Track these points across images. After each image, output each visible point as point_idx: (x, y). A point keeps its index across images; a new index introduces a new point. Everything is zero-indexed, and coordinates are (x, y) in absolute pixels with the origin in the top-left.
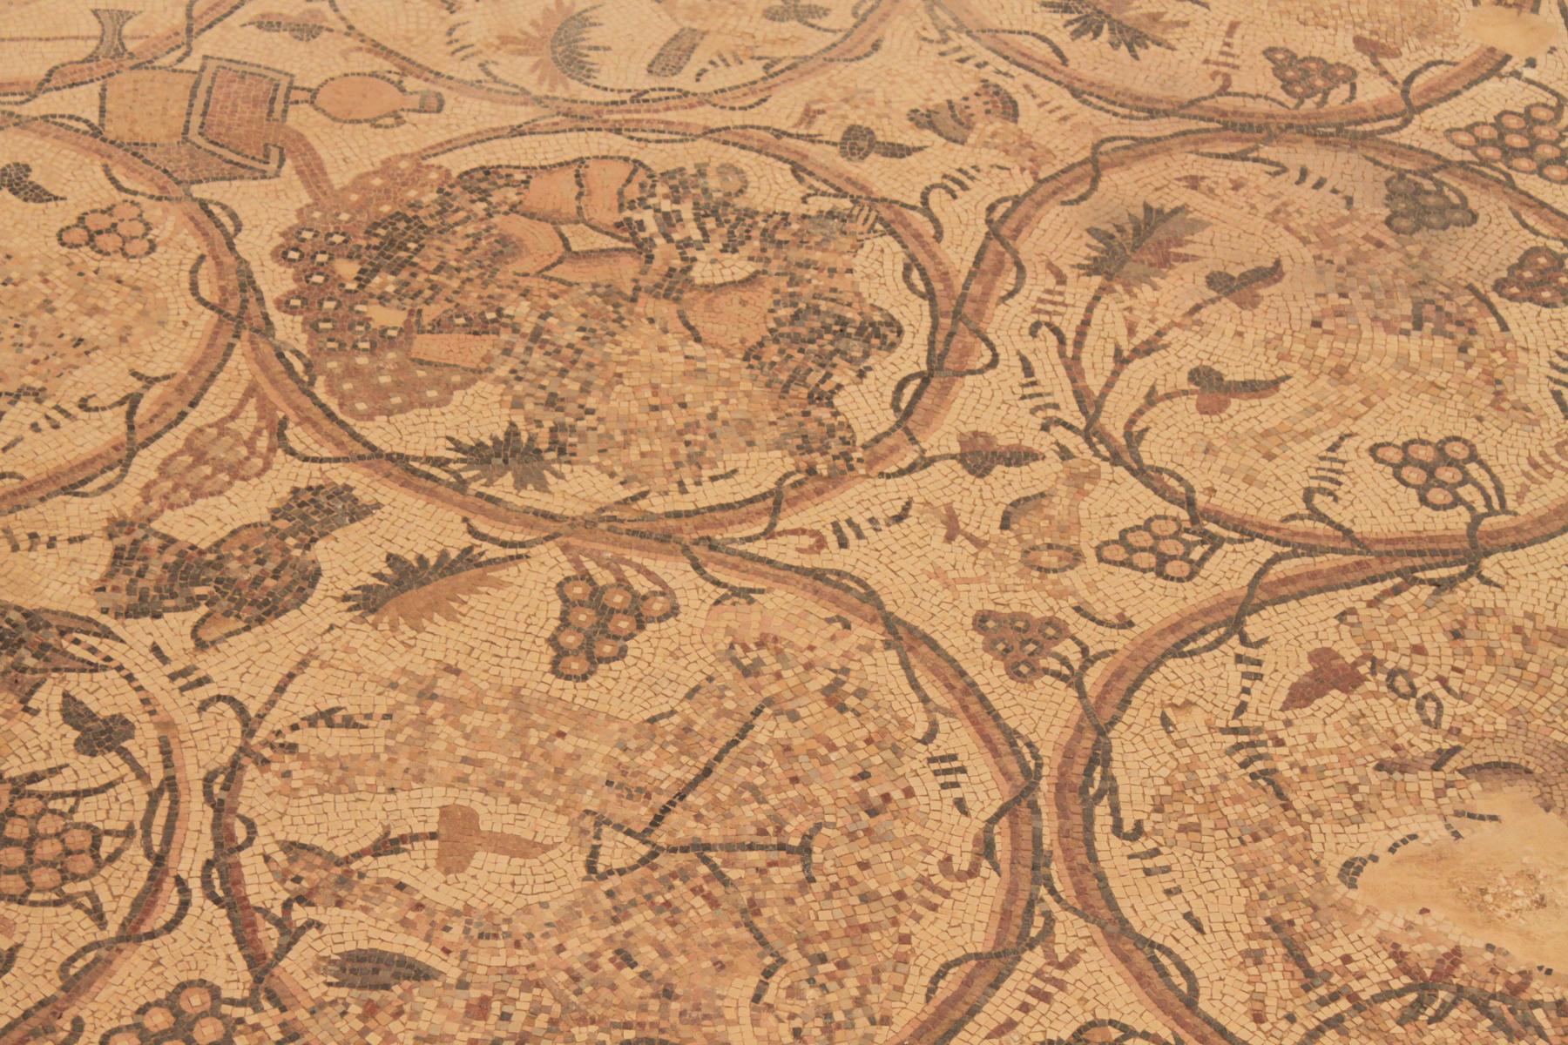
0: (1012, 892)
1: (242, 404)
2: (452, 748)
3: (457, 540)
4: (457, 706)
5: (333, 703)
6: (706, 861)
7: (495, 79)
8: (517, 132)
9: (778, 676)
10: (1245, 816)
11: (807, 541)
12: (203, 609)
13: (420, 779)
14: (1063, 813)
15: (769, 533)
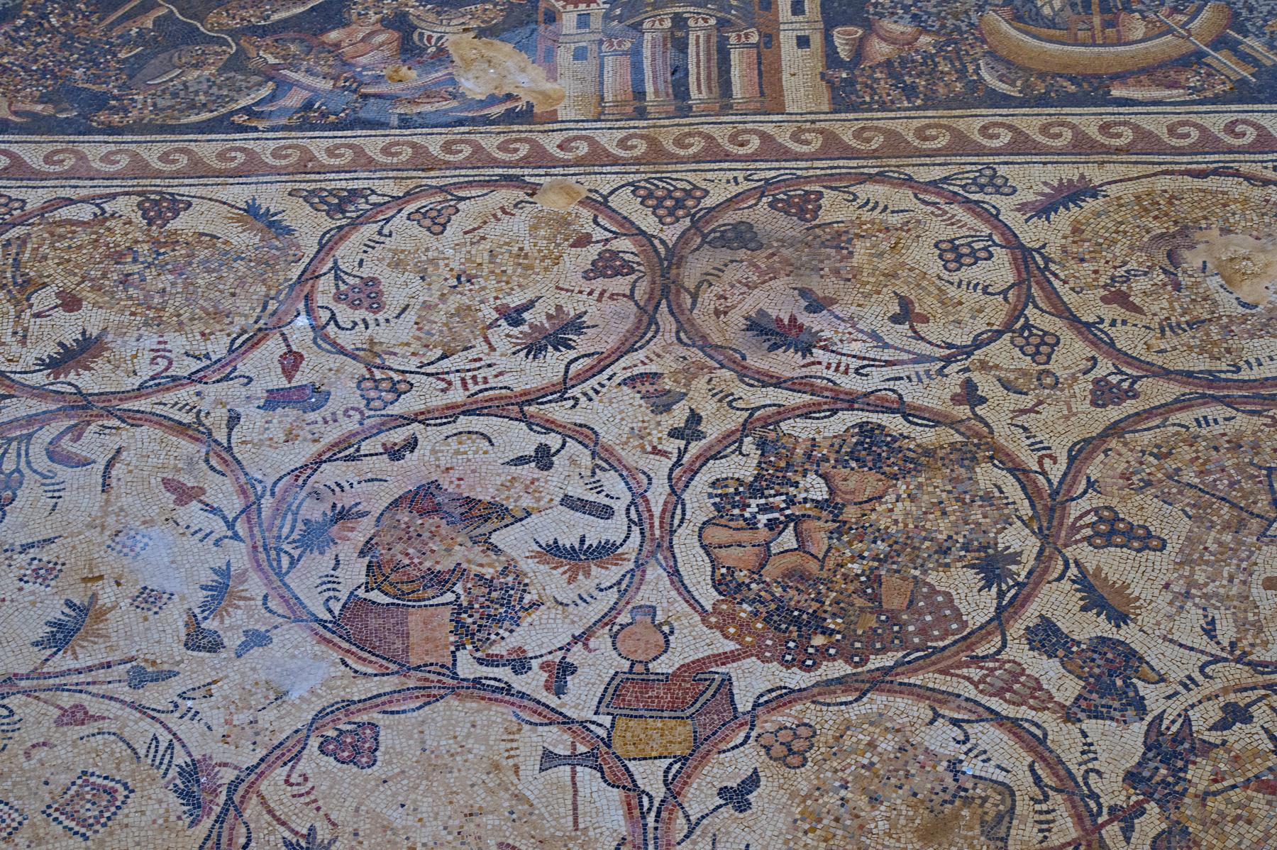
1: (958, 676)
2: (1224, 586)
3: (1066, 585)
4: (1191, 583)
7: (619, 583)
8: (675, 573)
9: (1149, 474)
10: (1218, 334)
11: (1047, 461)
12: (1134, 680)
13: (1247, 597)
14: (1229, 388)
15: (1044, 473)
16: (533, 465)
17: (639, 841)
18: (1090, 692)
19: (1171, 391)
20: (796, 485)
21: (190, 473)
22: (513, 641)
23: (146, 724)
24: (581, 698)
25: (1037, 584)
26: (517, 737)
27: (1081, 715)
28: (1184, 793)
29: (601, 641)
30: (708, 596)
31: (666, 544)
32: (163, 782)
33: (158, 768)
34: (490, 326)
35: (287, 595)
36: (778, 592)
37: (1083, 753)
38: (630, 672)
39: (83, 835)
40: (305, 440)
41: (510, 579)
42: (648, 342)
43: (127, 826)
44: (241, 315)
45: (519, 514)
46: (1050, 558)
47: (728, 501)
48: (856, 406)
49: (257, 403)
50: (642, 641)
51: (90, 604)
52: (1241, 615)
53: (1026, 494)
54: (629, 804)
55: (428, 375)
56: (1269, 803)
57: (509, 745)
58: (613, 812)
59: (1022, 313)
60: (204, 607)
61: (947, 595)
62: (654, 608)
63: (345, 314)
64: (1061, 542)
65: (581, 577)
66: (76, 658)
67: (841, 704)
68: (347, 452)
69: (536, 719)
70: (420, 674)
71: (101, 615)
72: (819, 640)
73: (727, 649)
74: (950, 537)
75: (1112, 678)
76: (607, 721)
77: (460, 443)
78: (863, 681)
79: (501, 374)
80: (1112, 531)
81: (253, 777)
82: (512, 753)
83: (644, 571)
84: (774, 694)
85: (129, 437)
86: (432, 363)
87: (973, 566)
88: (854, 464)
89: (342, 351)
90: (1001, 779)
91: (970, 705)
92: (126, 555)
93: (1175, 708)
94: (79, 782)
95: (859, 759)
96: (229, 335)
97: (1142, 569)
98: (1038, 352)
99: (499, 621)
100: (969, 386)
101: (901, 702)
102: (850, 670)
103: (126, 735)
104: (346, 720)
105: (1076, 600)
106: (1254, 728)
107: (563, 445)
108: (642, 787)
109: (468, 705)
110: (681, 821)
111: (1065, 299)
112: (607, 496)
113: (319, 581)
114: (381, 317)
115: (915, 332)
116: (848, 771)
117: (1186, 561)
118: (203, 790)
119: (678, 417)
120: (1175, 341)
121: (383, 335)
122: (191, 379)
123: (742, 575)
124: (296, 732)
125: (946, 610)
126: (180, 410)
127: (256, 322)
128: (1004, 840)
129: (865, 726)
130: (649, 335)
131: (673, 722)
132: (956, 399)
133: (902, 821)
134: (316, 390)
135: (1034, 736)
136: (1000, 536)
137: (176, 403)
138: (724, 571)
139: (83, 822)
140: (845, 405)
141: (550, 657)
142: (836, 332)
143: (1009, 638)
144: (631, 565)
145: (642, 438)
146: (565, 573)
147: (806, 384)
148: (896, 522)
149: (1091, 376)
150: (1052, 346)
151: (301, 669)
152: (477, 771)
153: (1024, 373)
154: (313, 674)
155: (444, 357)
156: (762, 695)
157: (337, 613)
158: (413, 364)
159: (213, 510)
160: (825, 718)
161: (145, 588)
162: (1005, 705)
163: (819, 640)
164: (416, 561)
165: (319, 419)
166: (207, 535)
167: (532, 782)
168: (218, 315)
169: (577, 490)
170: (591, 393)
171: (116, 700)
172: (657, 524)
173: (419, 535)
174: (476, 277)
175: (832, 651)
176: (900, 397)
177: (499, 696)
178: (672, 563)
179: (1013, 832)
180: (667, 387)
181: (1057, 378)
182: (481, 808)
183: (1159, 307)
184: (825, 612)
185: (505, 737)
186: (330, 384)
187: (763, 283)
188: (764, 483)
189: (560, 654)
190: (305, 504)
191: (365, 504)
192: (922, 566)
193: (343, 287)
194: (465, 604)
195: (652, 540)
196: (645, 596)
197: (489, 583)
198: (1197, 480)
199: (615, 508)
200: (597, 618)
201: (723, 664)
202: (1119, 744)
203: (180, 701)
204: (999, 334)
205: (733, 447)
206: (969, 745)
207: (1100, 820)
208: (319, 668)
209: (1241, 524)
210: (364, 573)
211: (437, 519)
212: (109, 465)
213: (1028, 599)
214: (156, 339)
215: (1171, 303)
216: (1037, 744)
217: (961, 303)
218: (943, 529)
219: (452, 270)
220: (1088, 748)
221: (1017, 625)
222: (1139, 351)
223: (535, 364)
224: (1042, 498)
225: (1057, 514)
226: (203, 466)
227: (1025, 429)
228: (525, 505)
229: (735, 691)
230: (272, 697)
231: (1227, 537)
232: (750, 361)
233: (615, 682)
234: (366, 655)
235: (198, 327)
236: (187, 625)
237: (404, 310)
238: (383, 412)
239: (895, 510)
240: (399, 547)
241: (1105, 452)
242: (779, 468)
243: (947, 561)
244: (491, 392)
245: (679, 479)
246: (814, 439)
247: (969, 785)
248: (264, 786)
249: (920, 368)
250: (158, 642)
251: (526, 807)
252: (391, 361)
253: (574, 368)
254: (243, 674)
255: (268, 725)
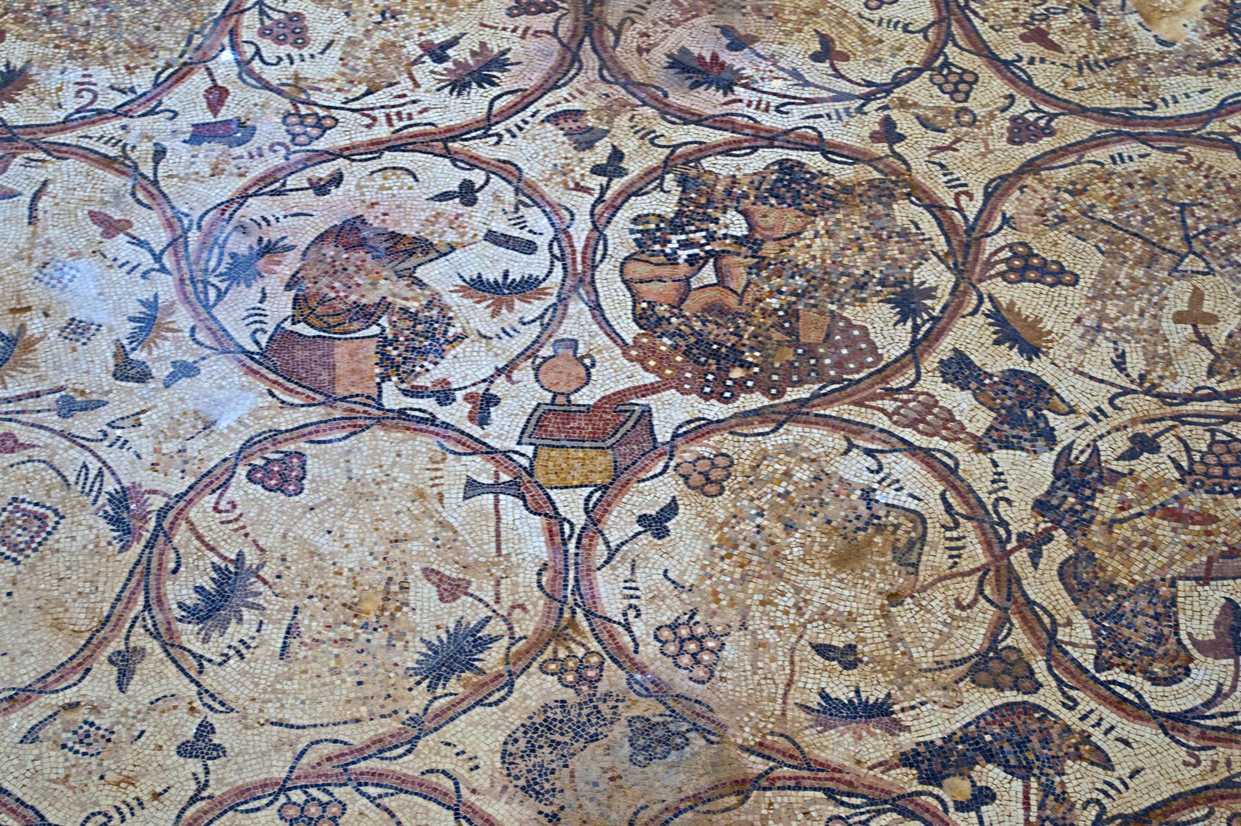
0: (1196, 143)
1: (872, 407)
2: (1135, 320)
4: (1103, 317)
5: (1109, 362)
6: (1195, 236)
7: (542, 317)
9: (1064, 210)
10: (1135, 71)
11: (963, 198)
12: (1045, 412)
13: (1157, 331)
14: (1144, 125)
15: (960, 210)
16: (457, 200)
17: (560, 566)
18: (1002, 423)
19: (1088, 128)
20: (716, 221)
21: (117, 206)
22: (437, 373)
23: (75, 452)
24: (504, 429)
25: (952, 318)
26: (441, 466)
27: (992, 446)
28: (1091, 520)
29: (524, 373)
30: (629, 330)
31: (588, 279)
32: (93, 508)
33: (88, 495)
34: (415, 63)
35: (215, 327)
36: (698, 326)
37: (993, 482)
38: (553, 403)
39: (14, 560)
40: (231, 174)
41: (434, 312)
42: (571, 79)
43: (58, 551)
44: (165, 49)
45: (444, 249)
46: (965, 293)
47: (649, 236)
48: (776, 143)
49: (183, 137)
50: (563, 373)
51: (19, 334)
52: (1151, 348)
53: (942, 230)
54: (550, 531)
55: (353, 111)
56: (1174, 530)
57: (434, 474)
58: (535, 539)
59: (941, 52)
60: (132, 338)
61: (864, 329)
62: (576, 342)
63: (270, 49)
64: (976, 277)
65: (504, 311)
66: (5, 388)
67: (758, 434)
68: (273, 187)
69: (459, 449)
70: (346, 405)
71: (30, 345)
72: (737, 373)
73: (647, 382)
74: (867, 273)
75: (1023, 410)
76: (529, 450)
77: (385, 178)
78: (779, 413)
79: (425, 110)
80: (1026, 266)
81: (182, 504)
82: (437, 481)
83: (566, 306)
84: (693, 425)
85: (53, 168)
86: (357, 99)
87: (888, 301)
88: (773, 201)
89: (267, 86)
90: (913, 507)
91: (883, 436)
92: (53, 286)
93: (1084, 438)
94: (10, 508)
95: (776, 488)
96: (154, 69)
97: (1055, 303)
98: (957, 90)
99: (424, 353)
100: (888, 123)
101: (817, 433)
102: (767, 402)
103: (56, 461)
104: (273, 449)
105: (989, 334)
106: (1162, 458)
107: (487, 182)
108: (564, 515)
109: (393, 435)
110: (601, 547)
111: (985, 37)
112: (530, 231)
113: (246, 314)
114: (306, 52)
115: (835, 70)
116: (764, 500)
117: (1098, 295)
118: (133, 517)
119: (601, 153)
120: (1092, 79)
121: (308, 70)
122: (117, 112)
123: (662, 310)
124: (225, 460)
125: (862, 345)
126: (106, 143)
127: (181, 56)
128: (915, 566)
129: (781, 456)
130: (573, 72)
131: (594, 452)
132: (875, 137)
133: (816, 548)
134: (241, 125)
135: (946, 465)
136: (916, 271)
137: (102, 137)
138: (644, 305)
139: (14, 547)
140: (766, 143)
141: (474, 389)
142: (758, 70)
143: (923, 371)
144: (553, 299)
145: (565, 174)
146: (488, 306)
147: (727, 122)
148: (814, 258)
149: (1008, 114)
150: (971, 84)
151: (229, 400)
152: (402, 499)
153: (942, 111)
154: (241, 404)
155: (369, 93)
156: (681, 426)
157: (264, 345)
158: (337, 100)
159: (141, 243)
160: (741, 448)
161: (73, 319)
162: (918, 436)
163: (737, 373)
164: (342, 294)
165: (245, 154)
166: (134, 268)
167: (456, 510)
168: (142, 48)
169: (501, 226)
170: (515, 130)
171: (46, 428)
172: (579, 259)
173: (345, 269)
174: (401, 13)
175: (750, 384)
176: (820, 134)
177: (424, 427)
178: (593, 298)
179: (924, 558)
180: (590, 124)
181: (975, 116)
182: (406, 535)
183: (1077, 45)
184: (744, 345)
185: (429, 466)
186: (256, 119)
187: (686, 20)
188: (685, 220)
189: (484, 386)
190: (232, 238)
191: (291, 238)
192: (839, 300)
193: (268, 22)
194: (390, 337)
195: (575, 275)
196: (567, 330)
197: (414, 317)
198: (1111, 216)
199: (539, 243)
200: (520, 350)
201: (643, 396)
202: (1028, 474)
203: (109, 430)
204: (918, 72)
205: (654, 184)
206: (882, 475)
207: (1009, 547)
208: (246, 398)
209: (1153, 260)
210: (290, 306)
211: (362, 253)
212: (36, 197)
213: (942, 332)
214: (80, 72)
215: (1089, 41)
216: (948, 473)
217: (881, 41)
218: (860, 264)
219: (376, 6)
220: (998, 478)
221: (931, 359)
222: (1057, 89)
223: (459, 101)
224: (958, 235)
225: (972, 250)
226: (129, 198)
227: (942, 166)
228: (449, 240)
229: (655, 422)
230: (200, 426)
231: (1139, 273)
232: (672, 99)
233: (537, 414)
234: (292, 386)
235: (123, 60)
236: (115, 356)
237: (329, 46)
238: (309, 148)
239: (813, 247)
240: (325, 280)
241: (1021, 189)
242: (700, 202)
243: (864, 295)
244: (416, 129)
245: (601, 215)
246: (734, 176)
247: (882, 513)
248: (193, 513)
249: (840, 106)
250: (87, 372)
251: (450, 533)
252: (316, 97)
253: (498, 105)
254: (171, 404)
255: (196, 454)
